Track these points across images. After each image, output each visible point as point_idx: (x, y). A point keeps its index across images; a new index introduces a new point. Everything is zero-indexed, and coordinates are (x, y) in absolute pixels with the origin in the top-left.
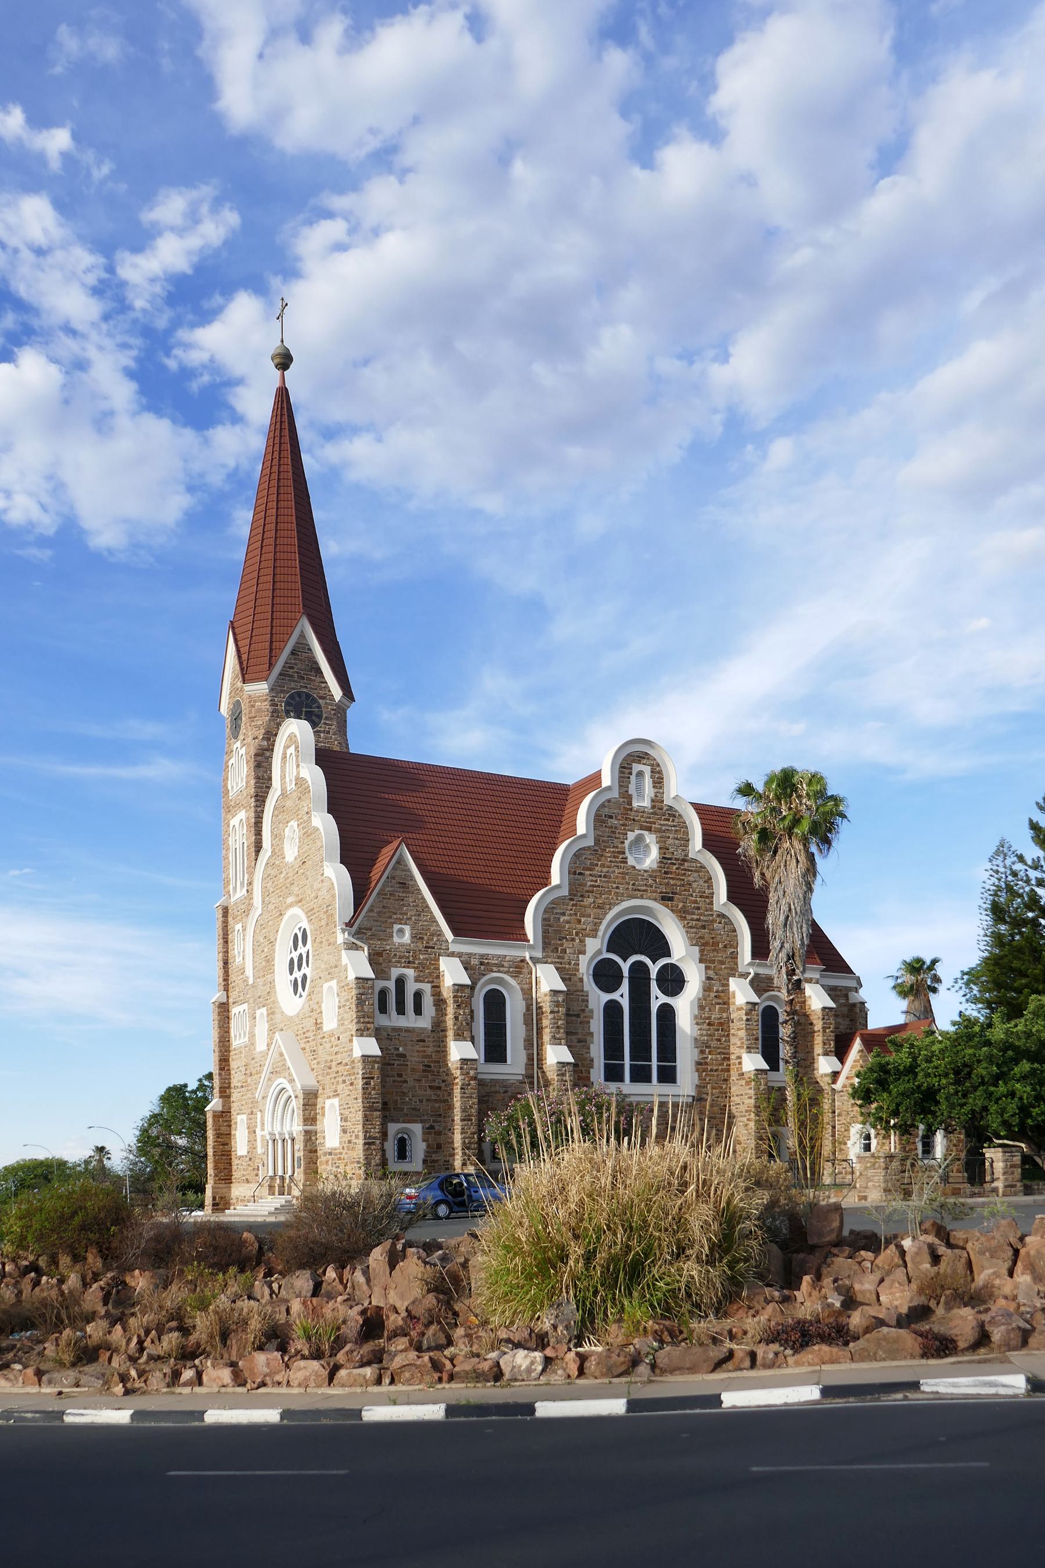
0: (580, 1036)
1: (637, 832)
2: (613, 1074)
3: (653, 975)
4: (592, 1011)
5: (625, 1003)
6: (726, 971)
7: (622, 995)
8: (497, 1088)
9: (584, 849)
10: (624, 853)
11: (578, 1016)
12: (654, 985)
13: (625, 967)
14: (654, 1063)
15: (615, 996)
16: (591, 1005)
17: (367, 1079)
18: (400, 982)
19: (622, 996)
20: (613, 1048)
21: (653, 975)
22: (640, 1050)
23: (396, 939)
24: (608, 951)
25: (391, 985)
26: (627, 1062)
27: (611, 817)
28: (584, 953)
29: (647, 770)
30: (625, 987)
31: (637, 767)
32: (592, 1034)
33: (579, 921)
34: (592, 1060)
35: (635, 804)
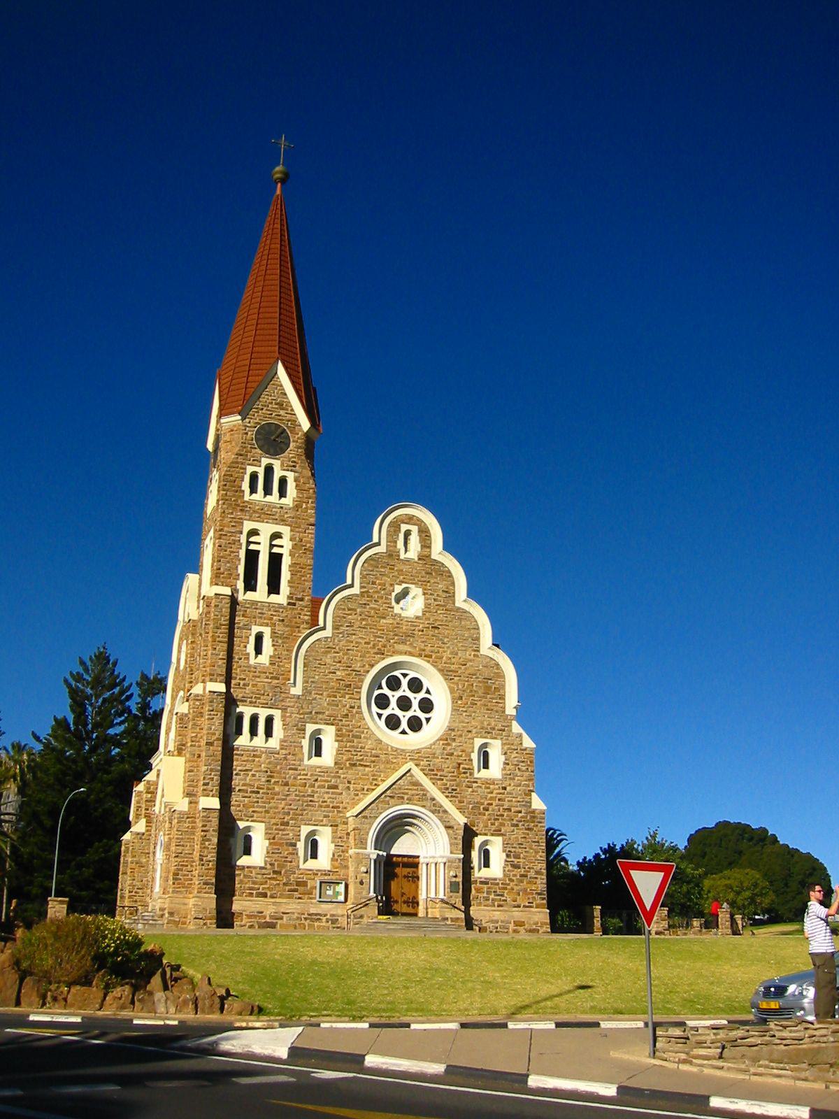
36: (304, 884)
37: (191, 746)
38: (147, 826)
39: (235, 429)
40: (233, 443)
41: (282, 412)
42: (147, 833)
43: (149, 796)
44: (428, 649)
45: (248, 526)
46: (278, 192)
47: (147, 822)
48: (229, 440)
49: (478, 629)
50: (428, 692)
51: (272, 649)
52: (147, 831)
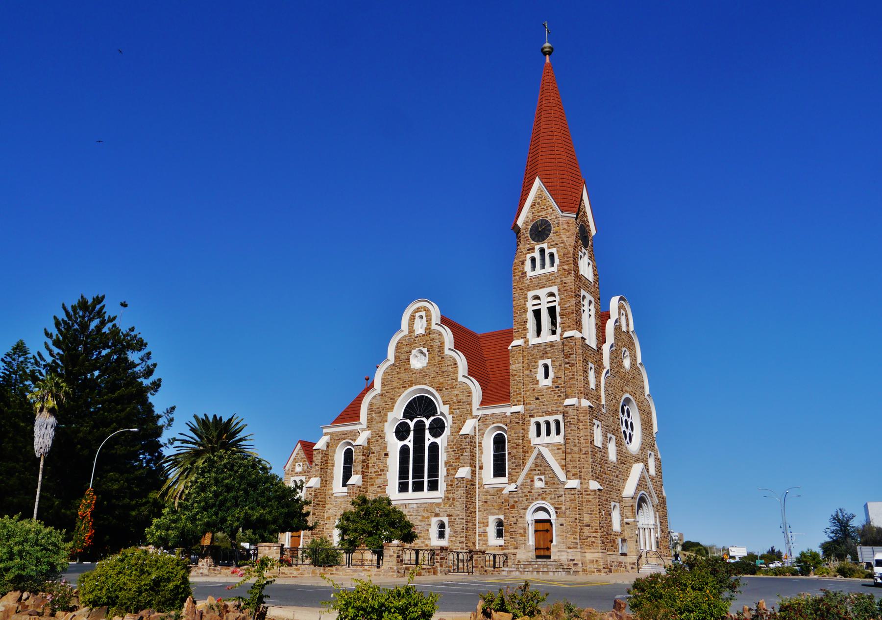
2: (403, 488)
3: (427, 426)
5: (411, 446)
7: (409, 442)
12: (427, 432)
13: (412, 424)
14: (426, 479)
15: (406, 442)
19: (410, 441)
20: (403, 473)
21: (427, 426)
22: (418, 472)
29: (423, 313)
30: (411, 437)
36: (614, 542)
37: (578, 443)
38: (363, 481)
39: (570, 222)
40: (570, 232)
41: (585, 219)
42: (363, 487)
43: (364, 458)
44: (634, 391)
45: (583, 292)
46: (548, 60)
47: (363, 478)
48: (567, 229)
49: (643, 382)
50: (631, 419)
51: (595, 379)
52: (363, 485)
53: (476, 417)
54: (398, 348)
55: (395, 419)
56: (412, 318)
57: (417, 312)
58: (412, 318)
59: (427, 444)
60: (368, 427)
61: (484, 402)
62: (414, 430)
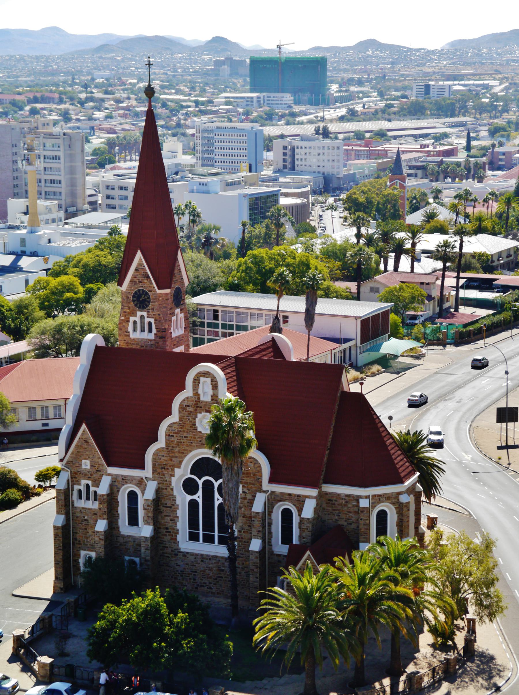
0: (172, 518)
1: (203, 413)
2: (193, 537)
4: (178, 505)
5: (200, 501)
6: (255, 489)
7: (199, 497)
8: (130, 539)
9: (174, 423)
10: (195, 425)
11: (171, 507)
13: (200, 482)
15: (195, 497)
16: (179, 502)
17: (56, 535)
18: (87, 486)
20: (193, 523)
23: (84, 467)
24: (191, 473)
25: (82, 488)
26: (201, 532)
27: (188, 406)
28: (173, 475)
29: (209, 380)
30: (200, 493)
31: (202, 379)
32: (178, 517)
33: (171, 460)
34: (178, 530)
35: (202, 399)
53: (264, 492)
54: (182, 408)
55: (183, 476)
56: (196, 381)
57: (201, 376)
58: (196, 381)
59: (217, 503)
60: (154, 477)
61: (272, 480)
62: (203, 488)
